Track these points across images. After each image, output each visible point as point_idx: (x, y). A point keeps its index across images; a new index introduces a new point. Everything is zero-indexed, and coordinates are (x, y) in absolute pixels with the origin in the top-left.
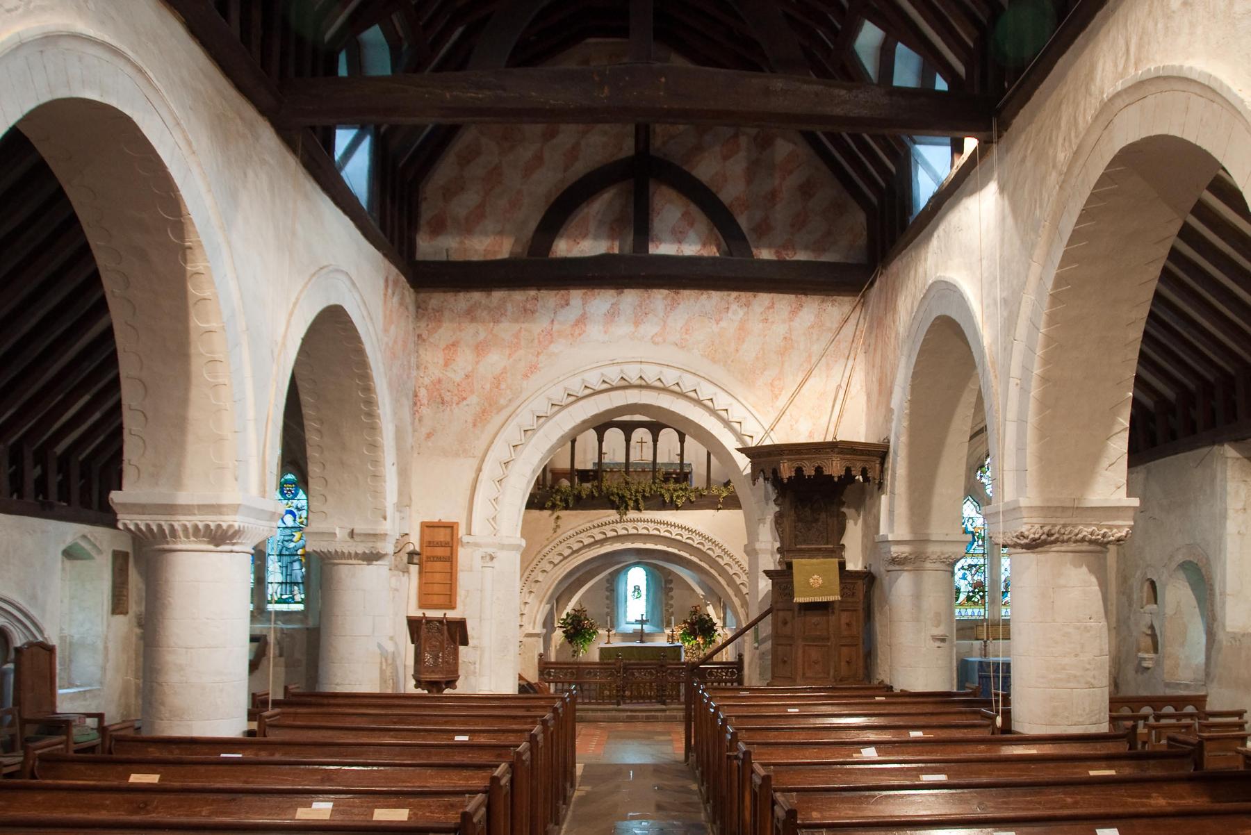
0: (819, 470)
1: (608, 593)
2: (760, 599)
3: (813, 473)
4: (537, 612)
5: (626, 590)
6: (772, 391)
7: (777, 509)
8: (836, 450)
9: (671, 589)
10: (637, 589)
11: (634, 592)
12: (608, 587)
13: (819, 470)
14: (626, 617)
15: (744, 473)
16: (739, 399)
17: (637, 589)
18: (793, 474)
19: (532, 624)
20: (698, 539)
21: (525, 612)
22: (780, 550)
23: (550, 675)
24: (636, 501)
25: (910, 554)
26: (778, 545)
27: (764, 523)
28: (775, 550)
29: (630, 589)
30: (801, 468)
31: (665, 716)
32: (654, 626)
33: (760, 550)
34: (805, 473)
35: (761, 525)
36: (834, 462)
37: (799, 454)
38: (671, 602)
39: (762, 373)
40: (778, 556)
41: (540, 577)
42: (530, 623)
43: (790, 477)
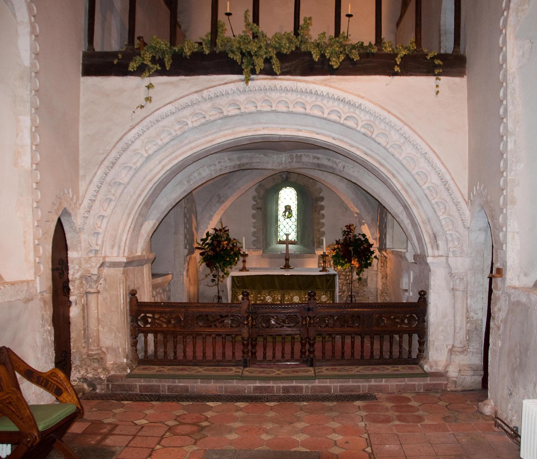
1: (254, 212)
4: (123, 231)
5: (277, 210)
9: (322, 208)
10: (288, 209)
11: (285, 212)
12: (254, 205)
14: (277, 236)
17: (288, 209)
19: (116, 249)
20: (363, 117)
21: (100, 231)
23: (146, 322)
24: (268, 61)
29: (281, 209)
31: (313, 387)
32: (304, 246)
38: (322, 221)
41: (124, 177)
42: (113, 247)
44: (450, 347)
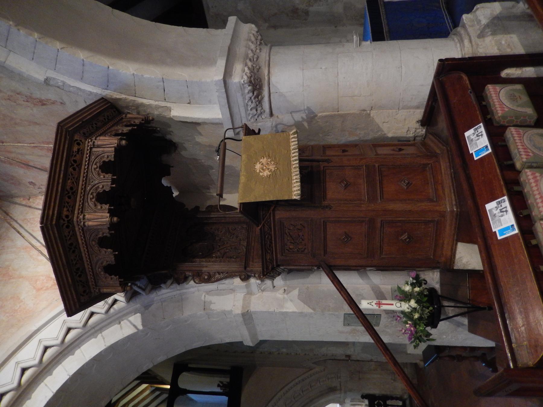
0: (106, 167)
2: (311, 311)
3: (109, 176)
6: (47, 289)
7: (192, 283)
8: (76, 137)
13: (106, 167)
15: (140, 327)
16: (34, 328)
18: (107, 206)
22: (245, 278)
25: (246, 65)
26: (237, 281)
27: (211, 303)
28: (243, 284)
30: (99, 194)
33: (243, 307)
34: (107, 189)
35: (213, 307)
36: (98, 142)
37: (75, 193)
39: (22, 301)
40: (253, 281)
43: (110, 211)
44: (392, 381)
